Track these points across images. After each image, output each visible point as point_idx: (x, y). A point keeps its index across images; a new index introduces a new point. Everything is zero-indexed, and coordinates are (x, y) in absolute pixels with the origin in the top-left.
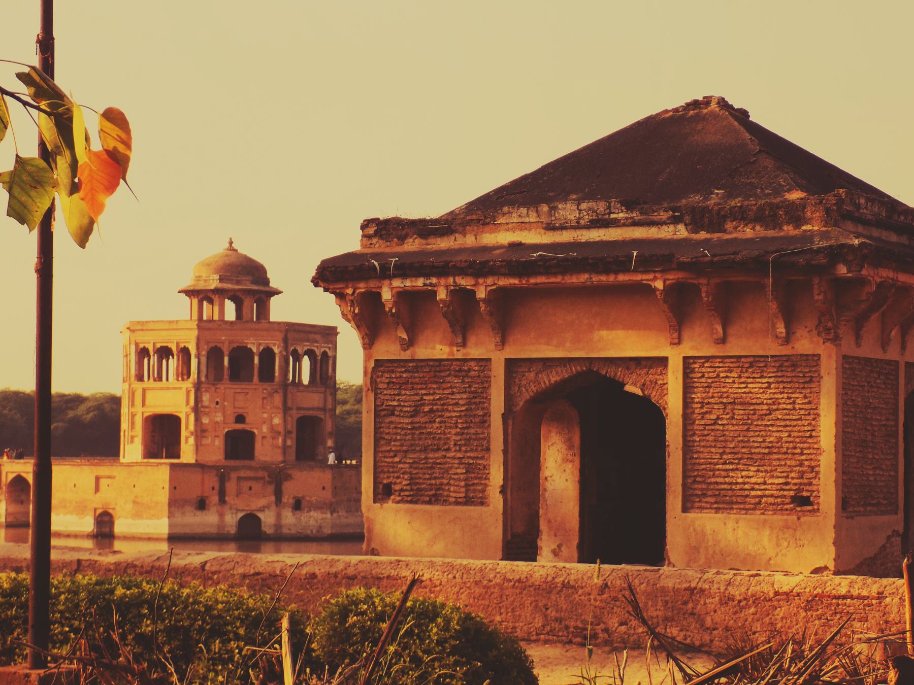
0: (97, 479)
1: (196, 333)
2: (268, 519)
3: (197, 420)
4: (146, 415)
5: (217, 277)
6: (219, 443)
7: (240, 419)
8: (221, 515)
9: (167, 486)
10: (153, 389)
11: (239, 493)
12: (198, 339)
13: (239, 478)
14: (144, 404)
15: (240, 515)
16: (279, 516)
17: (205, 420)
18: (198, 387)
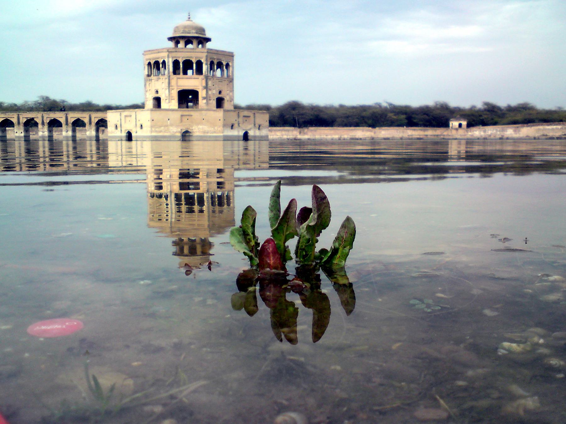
0: (182, 116)
1: (206, 54)
2: (251, 133)
3: (207, 92)
4: (179, 90)
5: (194, 31)
6: (214, 103)
7: (220, 92)
8: (239, 132)
9: (222, 120)
10: (183, 78)
11: (243, 122)
12: (207, 56)
13: (244, 116)
14: (177, 86)
15: (244, 132)
16: (255, 132)
17: (210, 92)
18: (207, 78)
